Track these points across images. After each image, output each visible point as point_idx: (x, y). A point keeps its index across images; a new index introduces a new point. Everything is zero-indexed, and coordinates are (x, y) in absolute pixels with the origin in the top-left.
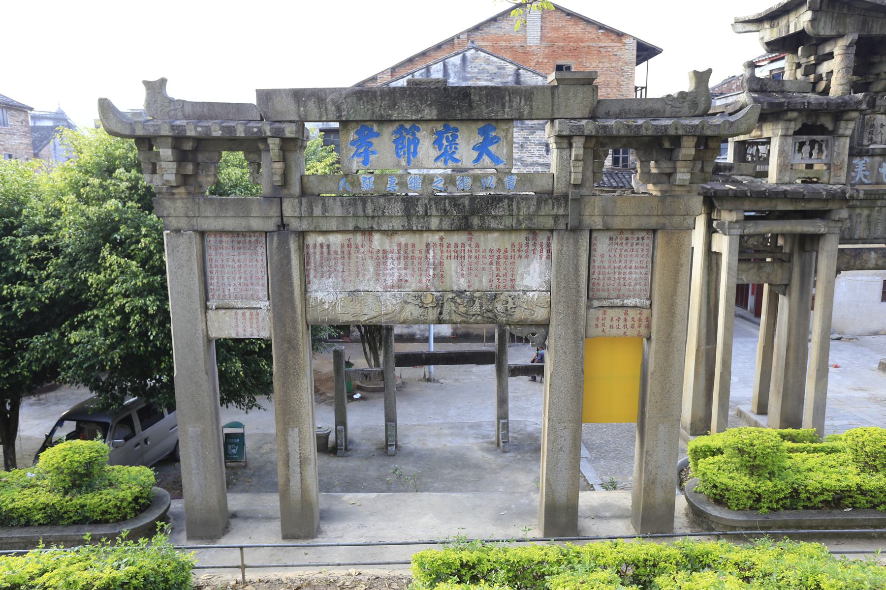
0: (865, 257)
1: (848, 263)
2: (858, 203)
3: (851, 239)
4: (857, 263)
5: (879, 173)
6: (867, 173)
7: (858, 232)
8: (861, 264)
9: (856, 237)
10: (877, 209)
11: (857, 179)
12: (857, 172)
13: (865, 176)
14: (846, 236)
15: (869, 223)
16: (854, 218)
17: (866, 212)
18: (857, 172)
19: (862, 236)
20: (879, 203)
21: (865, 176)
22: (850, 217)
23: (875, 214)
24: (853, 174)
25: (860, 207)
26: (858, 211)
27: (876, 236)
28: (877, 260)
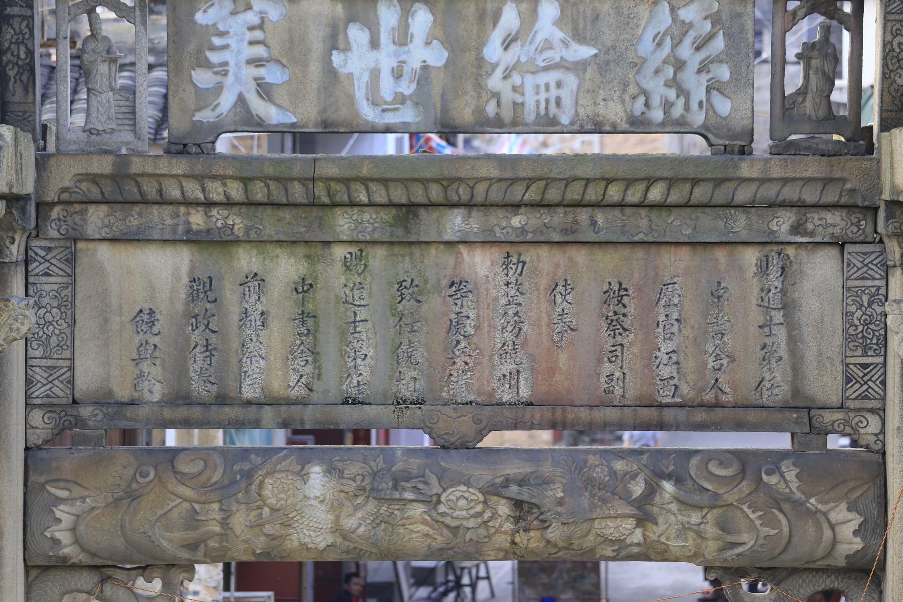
0: (273, 489)
1: (192, 521)
2: (238, 222)
3: (222, 400)
4: (240, 521)
5: (331, 74)
6: (274, 75)
7: (255, 367)
8: (257, 525)
9: (249, 391)
10: (340, 252)
11: (226, 101)
12: (222, 69)
13: (265, 90)
14: (199, 388)
15: (306, 319)
16: (230, 295)
17: (286, 268)
18: (222, 69)
19: (277, 387)
20: (343, 223)
21: (265, 90)
22: (202, 289)
23: (334, 276)
24: (203, 78)
25: (260, 243)
26: (246, 260)
27: (350, 387)
28: (335, 508)
